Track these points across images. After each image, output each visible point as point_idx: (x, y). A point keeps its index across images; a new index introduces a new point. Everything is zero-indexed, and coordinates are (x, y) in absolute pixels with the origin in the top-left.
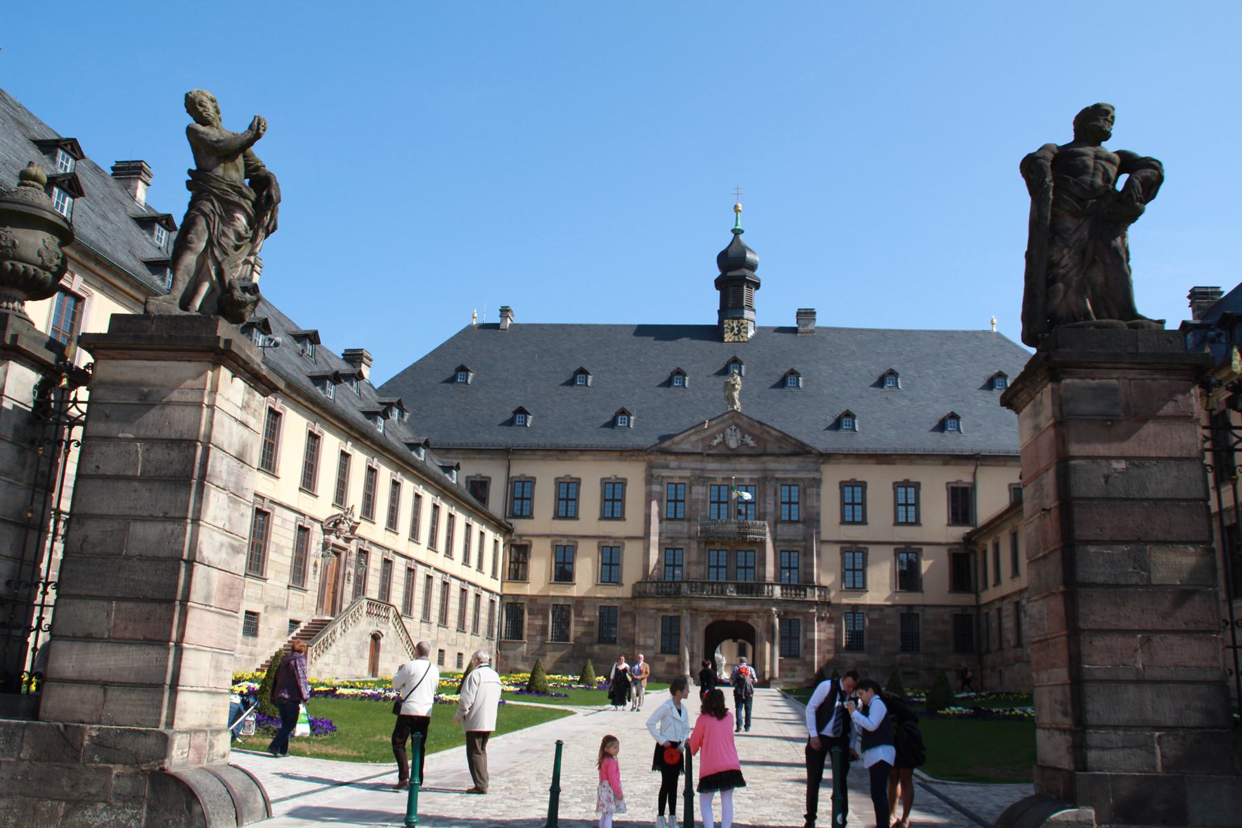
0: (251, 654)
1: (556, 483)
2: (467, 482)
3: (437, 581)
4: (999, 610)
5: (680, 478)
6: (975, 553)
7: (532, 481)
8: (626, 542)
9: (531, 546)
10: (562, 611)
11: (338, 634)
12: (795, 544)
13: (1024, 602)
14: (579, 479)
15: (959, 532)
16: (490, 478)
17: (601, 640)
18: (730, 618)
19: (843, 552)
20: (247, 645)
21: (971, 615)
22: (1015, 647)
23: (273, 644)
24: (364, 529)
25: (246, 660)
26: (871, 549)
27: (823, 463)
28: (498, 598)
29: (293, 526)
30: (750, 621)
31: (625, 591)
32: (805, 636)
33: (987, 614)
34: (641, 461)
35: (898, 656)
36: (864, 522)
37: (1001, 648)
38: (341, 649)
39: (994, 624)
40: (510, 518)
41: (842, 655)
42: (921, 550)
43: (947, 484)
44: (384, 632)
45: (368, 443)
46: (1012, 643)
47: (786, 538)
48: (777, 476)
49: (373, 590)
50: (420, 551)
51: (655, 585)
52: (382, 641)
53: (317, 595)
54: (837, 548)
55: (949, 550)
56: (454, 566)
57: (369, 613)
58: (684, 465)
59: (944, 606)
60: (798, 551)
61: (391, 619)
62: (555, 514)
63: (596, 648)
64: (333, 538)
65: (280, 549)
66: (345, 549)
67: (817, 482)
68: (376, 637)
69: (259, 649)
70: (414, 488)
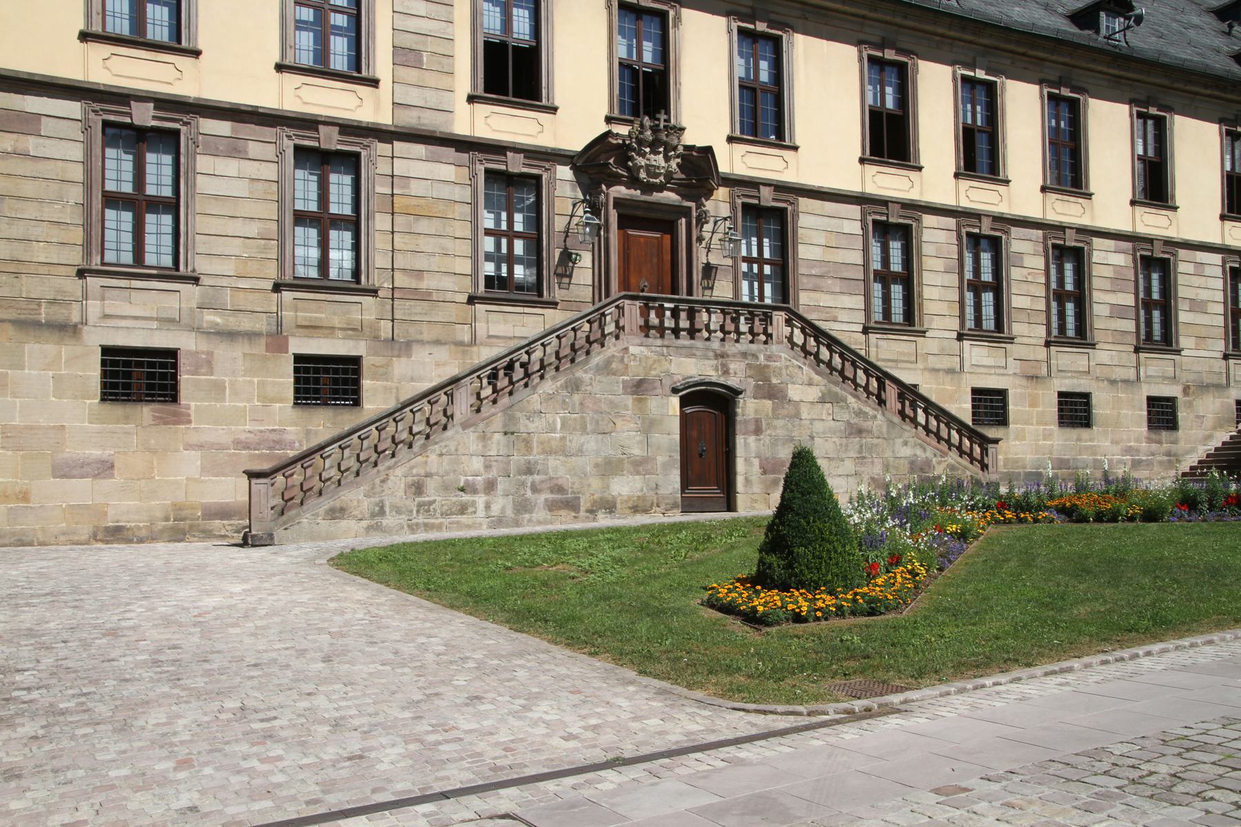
0: (1168, 454)
20: (1160, 442)
25: (1161, 463)
69: (1182, 445)
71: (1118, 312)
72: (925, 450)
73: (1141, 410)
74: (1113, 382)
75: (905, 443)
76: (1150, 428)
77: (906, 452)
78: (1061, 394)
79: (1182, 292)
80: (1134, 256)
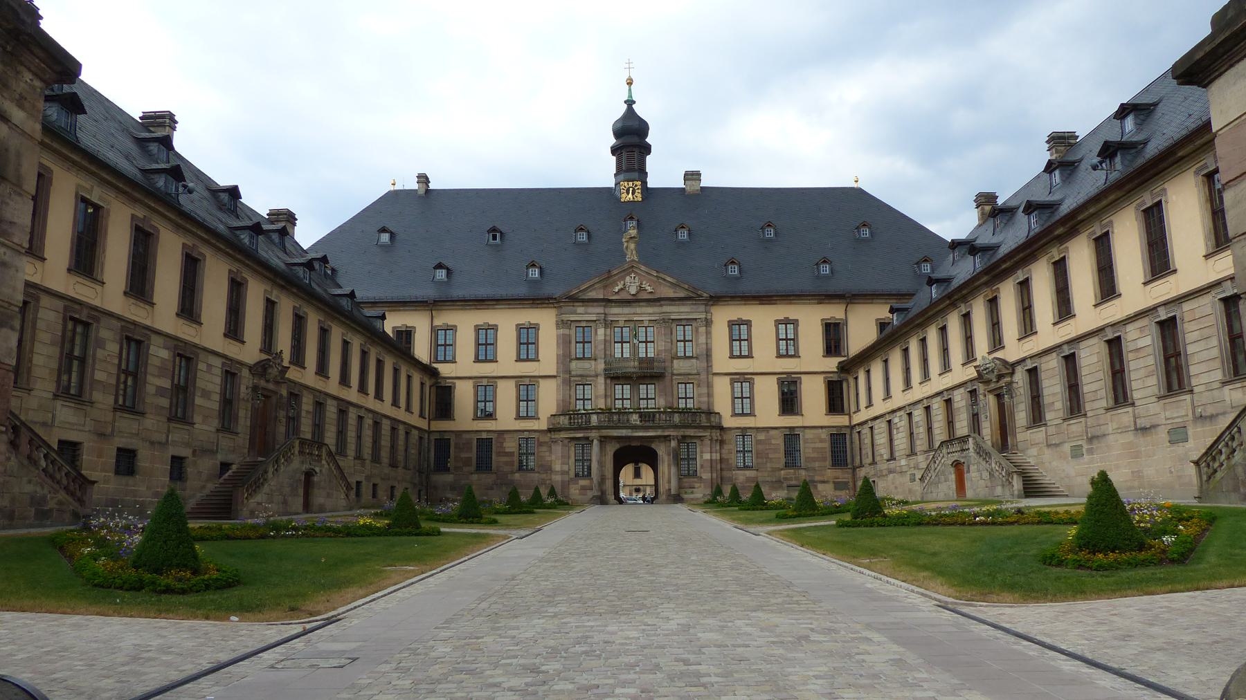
1: (475, 330)
2: (393, 332)
3: (368, 421)
4: (871, 428)
5: (587, 321)
6: (847, 380)
7: (453, 328)
8: (540, 380)
9: (455, 387)
10: (485, 445)
11: (270, 475)
12: (690, 377)
13: (896, 420)
14: (496, 326)
15: (832, 364)
16: (415, 328)
17: (520, 468)
18: (634, 444)
19: (733, 382)
21: (845, 434)
22: (888, 460)
23: (203, 487)
24: (293, 374)
26: (755, 377)
27: (712, 305)
28: (426, 435)
29: (218, 371)
30: (653, 446)
31: (542, 425)
32: (701, 457)
33: (859, 432)
34: (551, 307)
35: (782, 472)
36: (750, 356)
37: (874, 463)
38: (274, 488)
39: (867, 441)
40: (434, 363)
41: (734, 472)
42: (800, 378)
43: (822, 320)
44: (317, 469)
45: (295, 290)
46: (886, 457)
47: (682, 371)
48: (672, 317)
49: (306, 430)
50: (352, 395)
51: (567, 417)
52: (316, 479)
53: (249, 437)
54: (727, 379)
55: (825, 378)
56: (385, 408)
57: (301, 452)
58: (590, 310)
59: (822, 427)
60: (693, 383)
61: (323, 457)
62: (475, 358)
63: (517, 476)
64: (263, 383)
65: (206, 394)
66: (276, 393)
67: (708, 323)
68: (309, 475)
70: (343, 334)
71: (160, 391)
72: (43, 488)
73: (166, 465)
74: (152, 443)
75: (30, 482)
76: (171, 478)
77: (29, 488)
78: (119, 449)
79: (199, 383)
80: (174, 352)
